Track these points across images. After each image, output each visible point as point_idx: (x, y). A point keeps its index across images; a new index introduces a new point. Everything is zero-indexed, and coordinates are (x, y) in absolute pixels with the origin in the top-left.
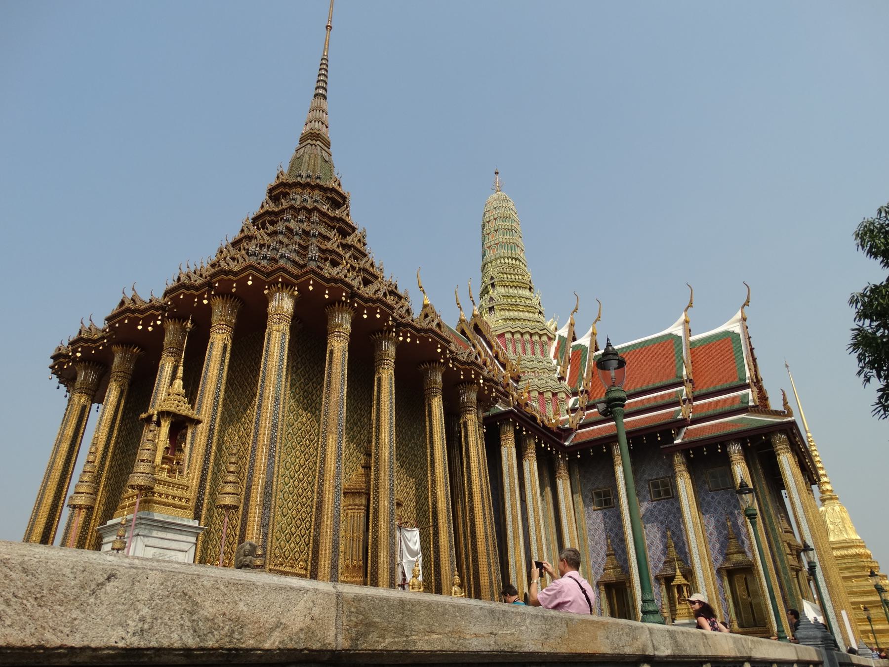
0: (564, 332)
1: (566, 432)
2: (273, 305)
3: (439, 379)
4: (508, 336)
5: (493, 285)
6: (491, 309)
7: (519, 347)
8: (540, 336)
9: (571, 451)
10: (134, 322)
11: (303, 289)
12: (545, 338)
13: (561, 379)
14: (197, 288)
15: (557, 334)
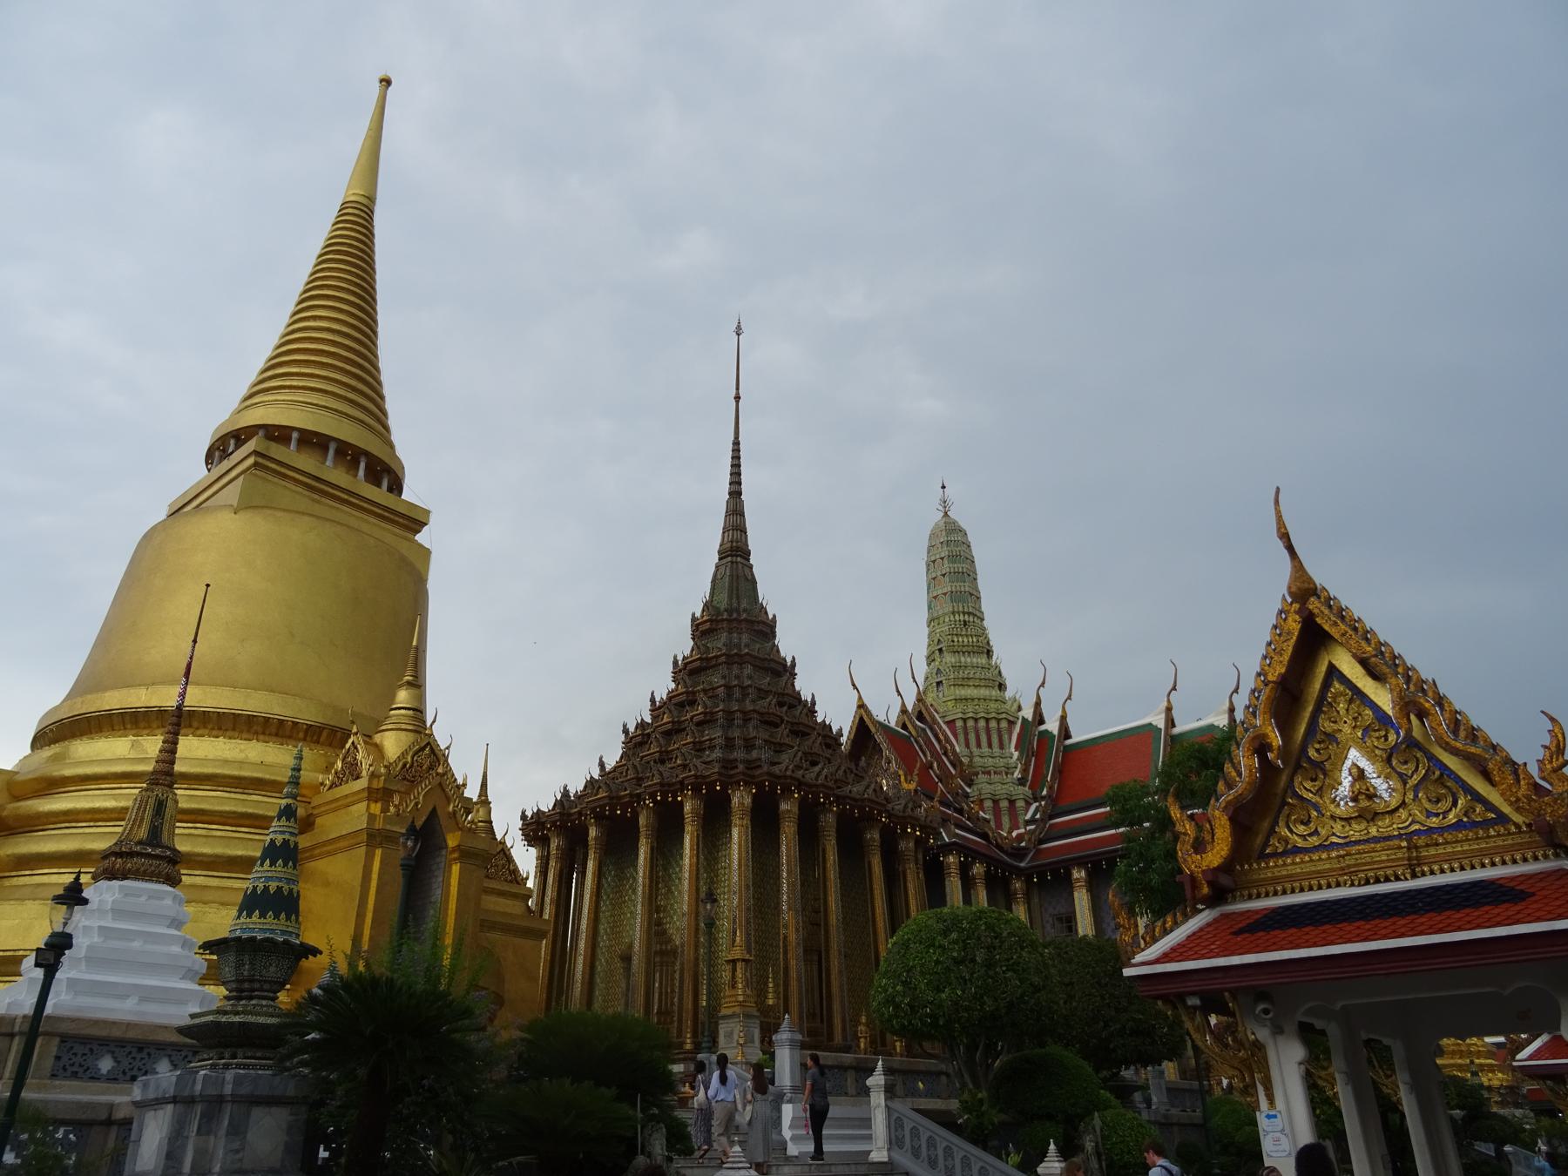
0: (1028, 713)
1: (1019, 854)
2: (735, 801)
3: (877, 836)
4: (959, 724)
5: (940, 650)
6: (939, 683)
7: (972, 737)
8: (999, 721)
9: (1026, 875)
10: (613, 810)
11: (760, 786)
12: (1004, 724)
13: (1021, 782)
14: (670, 785)
15: (1021, 714)
